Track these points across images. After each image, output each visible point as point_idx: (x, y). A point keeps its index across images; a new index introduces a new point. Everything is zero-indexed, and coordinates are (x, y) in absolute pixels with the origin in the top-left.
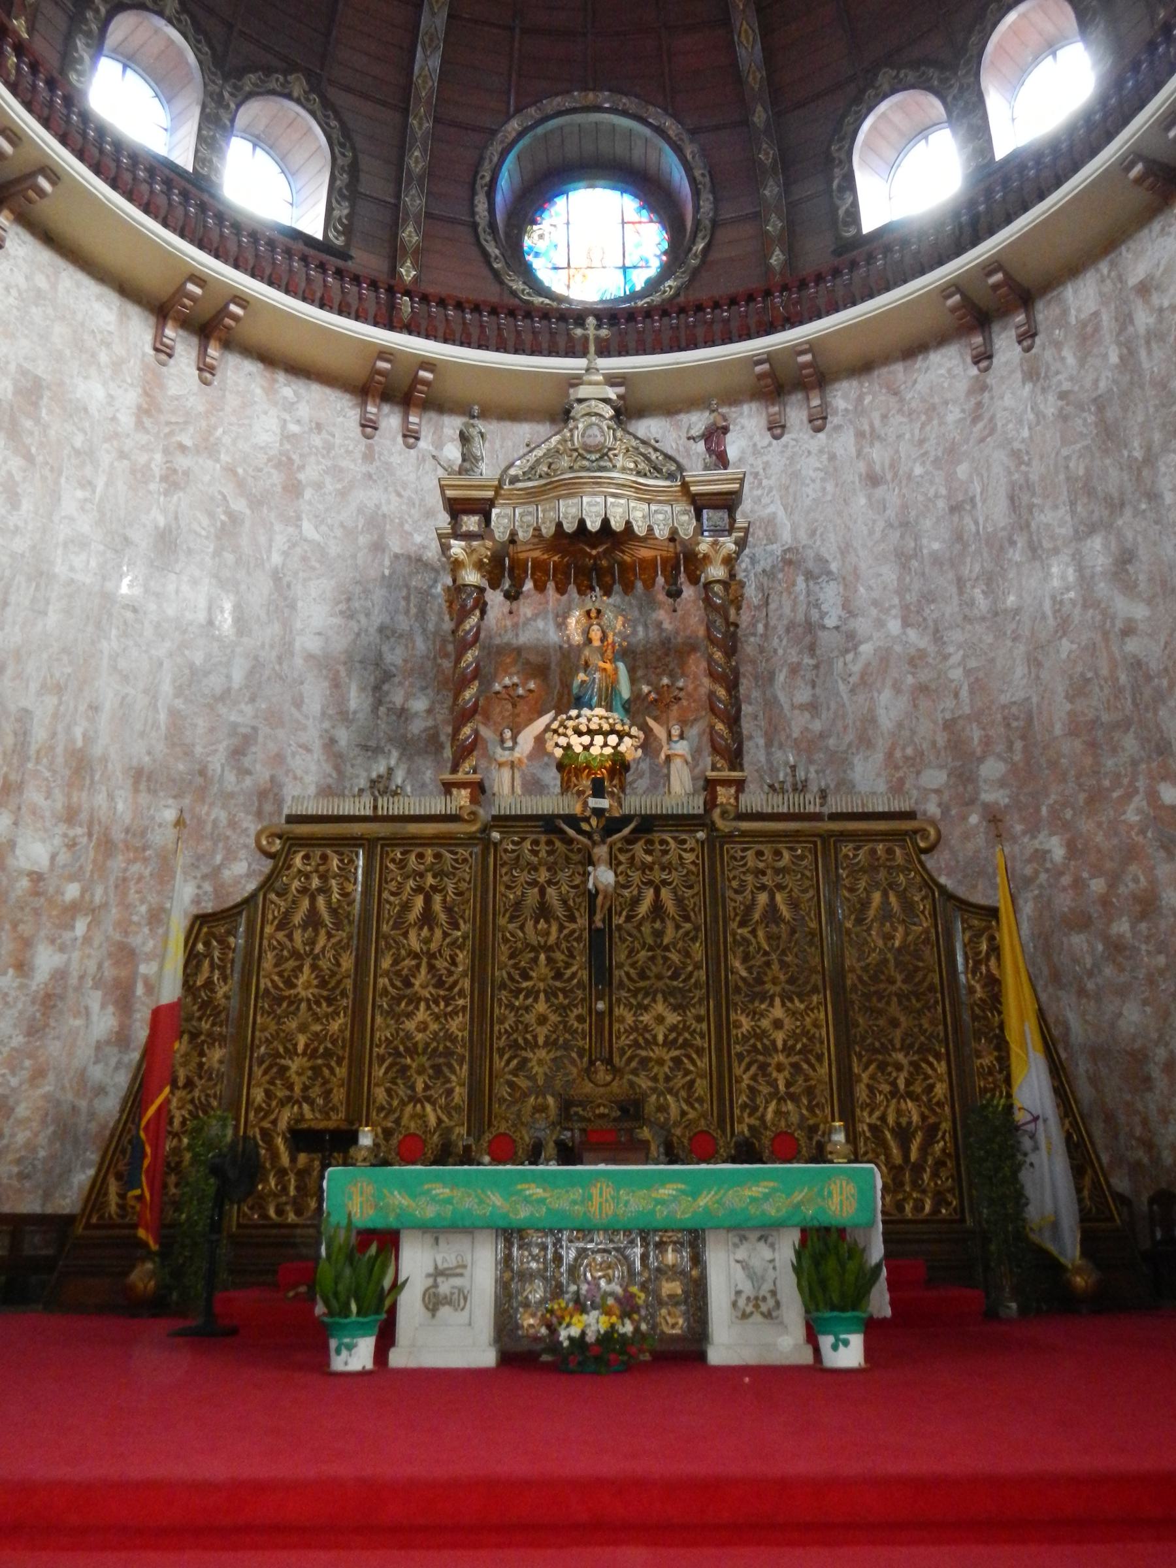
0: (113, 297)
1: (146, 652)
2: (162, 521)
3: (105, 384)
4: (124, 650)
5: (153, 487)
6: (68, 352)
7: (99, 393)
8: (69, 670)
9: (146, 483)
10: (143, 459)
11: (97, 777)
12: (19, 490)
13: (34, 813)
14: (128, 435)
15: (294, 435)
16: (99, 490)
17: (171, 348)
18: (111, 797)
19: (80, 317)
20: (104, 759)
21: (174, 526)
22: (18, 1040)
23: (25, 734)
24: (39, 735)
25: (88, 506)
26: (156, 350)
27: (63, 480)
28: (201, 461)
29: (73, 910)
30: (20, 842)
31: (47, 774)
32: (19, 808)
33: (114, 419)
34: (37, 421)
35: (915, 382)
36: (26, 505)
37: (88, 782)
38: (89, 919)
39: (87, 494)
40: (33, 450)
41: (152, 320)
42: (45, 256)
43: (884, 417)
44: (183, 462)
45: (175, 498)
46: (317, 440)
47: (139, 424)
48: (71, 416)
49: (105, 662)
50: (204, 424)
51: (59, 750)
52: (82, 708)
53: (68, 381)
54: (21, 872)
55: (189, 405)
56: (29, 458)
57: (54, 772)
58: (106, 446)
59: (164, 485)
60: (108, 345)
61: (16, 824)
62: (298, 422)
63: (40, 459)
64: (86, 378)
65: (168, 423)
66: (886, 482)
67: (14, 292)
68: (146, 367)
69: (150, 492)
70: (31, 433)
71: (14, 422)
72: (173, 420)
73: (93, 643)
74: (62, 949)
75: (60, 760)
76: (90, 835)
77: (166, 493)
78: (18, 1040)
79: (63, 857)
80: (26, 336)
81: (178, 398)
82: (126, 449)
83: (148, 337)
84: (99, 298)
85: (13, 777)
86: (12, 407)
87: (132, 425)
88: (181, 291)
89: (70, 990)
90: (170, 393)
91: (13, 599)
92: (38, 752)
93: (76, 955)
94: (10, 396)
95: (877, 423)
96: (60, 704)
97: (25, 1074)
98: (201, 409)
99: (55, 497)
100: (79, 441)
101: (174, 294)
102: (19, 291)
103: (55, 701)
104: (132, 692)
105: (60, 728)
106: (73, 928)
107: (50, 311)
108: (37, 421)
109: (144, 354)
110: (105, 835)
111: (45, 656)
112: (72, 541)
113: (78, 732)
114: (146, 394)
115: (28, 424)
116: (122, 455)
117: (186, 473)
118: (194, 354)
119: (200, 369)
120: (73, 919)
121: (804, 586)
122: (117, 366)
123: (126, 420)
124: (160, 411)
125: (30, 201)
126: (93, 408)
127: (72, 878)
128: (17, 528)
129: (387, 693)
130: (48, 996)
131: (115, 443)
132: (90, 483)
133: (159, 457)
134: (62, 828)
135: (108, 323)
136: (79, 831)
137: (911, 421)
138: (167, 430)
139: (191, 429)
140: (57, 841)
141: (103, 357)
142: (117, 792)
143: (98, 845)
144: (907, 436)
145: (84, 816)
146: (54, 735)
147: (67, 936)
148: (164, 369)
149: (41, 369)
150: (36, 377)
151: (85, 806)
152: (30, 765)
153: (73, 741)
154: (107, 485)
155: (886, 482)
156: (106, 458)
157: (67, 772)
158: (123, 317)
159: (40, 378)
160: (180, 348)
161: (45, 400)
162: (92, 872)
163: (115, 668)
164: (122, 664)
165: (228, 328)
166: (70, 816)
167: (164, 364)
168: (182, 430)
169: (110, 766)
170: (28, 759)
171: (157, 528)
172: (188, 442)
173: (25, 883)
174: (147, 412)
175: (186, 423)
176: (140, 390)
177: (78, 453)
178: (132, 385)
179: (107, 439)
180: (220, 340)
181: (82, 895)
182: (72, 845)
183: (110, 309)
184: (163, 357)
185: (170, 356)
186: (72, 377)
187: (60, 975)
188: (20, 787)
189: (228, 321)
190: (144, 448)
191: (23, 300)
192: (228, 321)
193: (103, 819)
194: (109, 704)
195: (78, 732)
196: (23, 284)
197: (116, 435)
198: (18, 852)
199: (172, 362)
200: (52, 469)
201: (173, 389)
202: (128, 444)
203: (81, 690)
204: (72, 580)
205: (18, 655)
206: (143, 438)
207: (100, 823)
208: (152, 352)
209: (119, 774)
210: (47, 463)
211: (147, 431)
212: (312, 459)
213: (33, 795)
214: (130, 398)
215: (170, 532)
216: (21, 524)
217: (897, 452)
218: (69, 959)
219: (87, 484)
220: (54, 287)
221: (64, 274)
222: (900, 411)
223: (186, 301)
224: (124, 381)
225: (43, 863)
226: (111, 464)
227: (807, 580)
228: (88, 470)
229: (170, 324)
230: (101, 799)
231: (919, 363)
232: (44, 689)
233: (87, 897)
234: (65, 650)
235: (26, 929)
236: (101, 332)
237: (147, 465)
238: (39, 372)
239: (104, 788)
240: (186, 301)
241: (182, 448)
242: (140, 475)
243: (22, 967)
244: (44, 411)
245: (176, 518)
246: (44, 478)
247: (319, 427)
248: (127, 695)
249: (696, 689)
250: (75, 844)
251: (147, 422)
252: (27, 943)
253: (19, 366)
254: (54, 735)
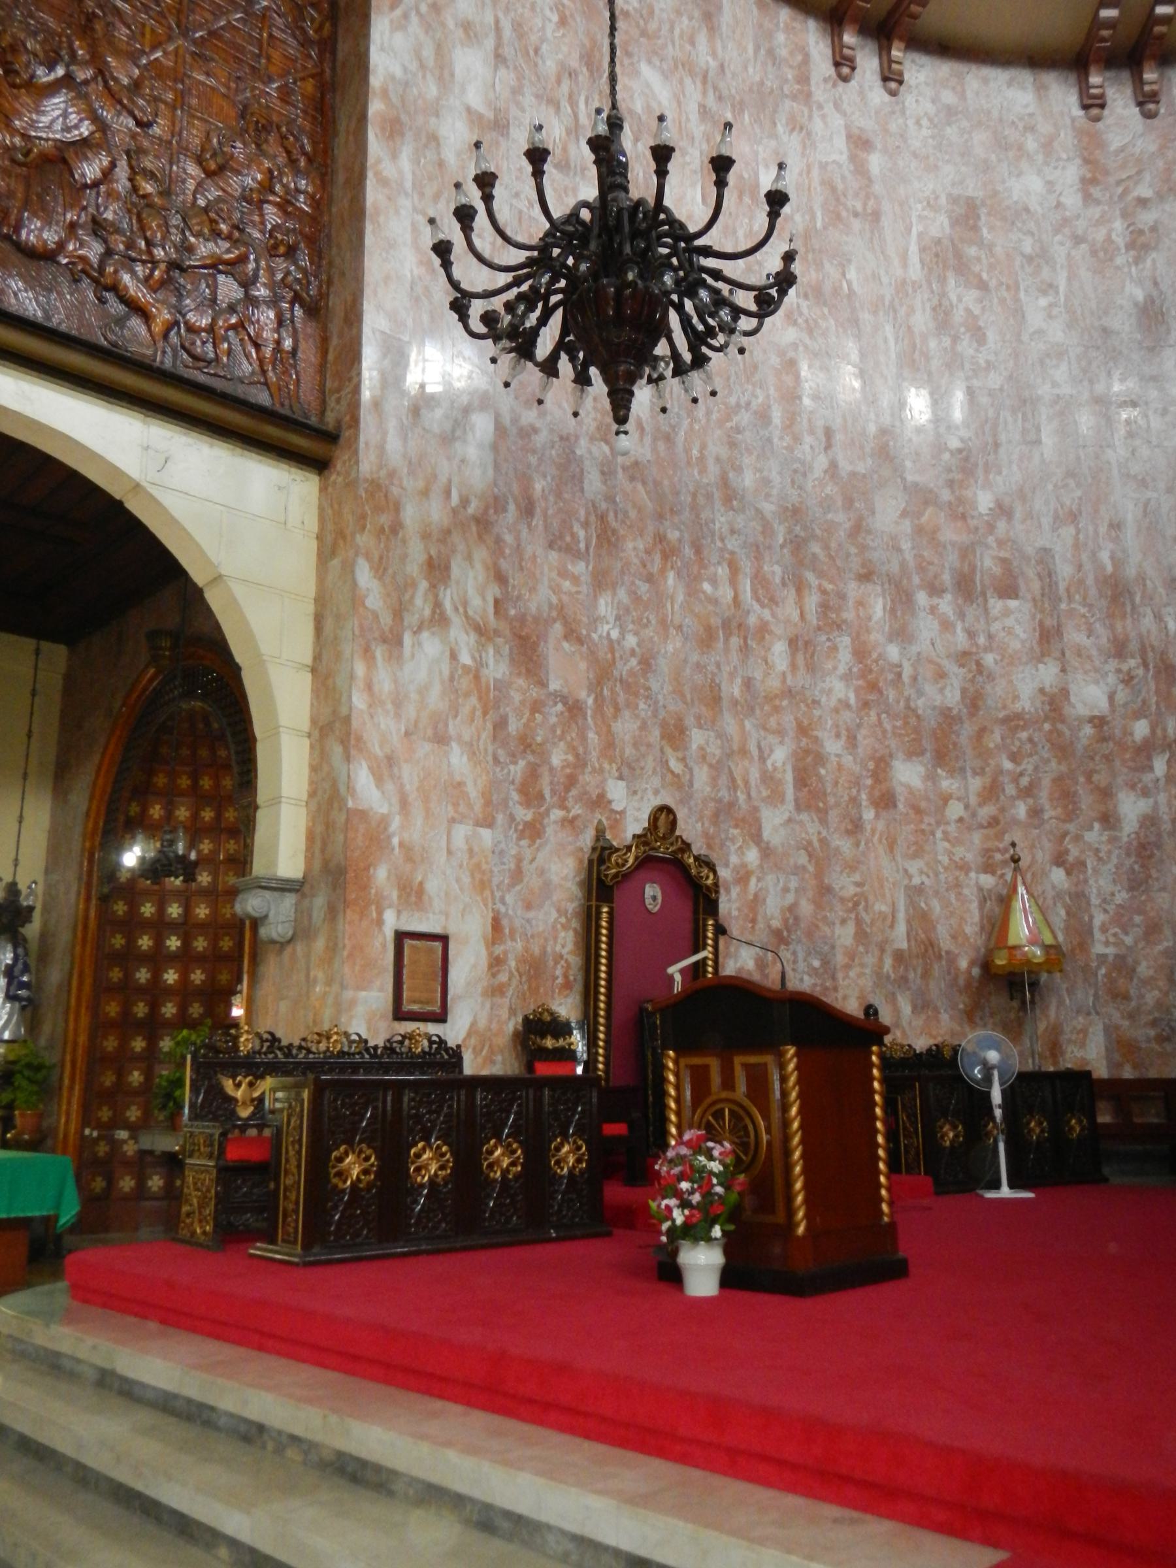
0: (1025, 76)
1: (1158, 446)
2: (1140, 295)
3: (1039, 172)
4: (1133, 452)
5: (1119, 261)
6: (993, 157)
7: (1035, 183)
8: (1079, 493)
9: (1111, 260)
10: (1100, 235)
11: (1138, 599)
12: (981, 323)
13: (1080, 656)
14: (1078, 217)
16: (1062, 289)
17: (1102, 96)
18: (1158, 617)
19: (995, 114)
20: (1142, 578)
21: (1155, 293)
22: (1122, 897)
23: (1050, 575)
24: (1064, 571)
25: (1055, 311)
26: (1085, 107)
27: (1022, 295)
28: (1167, 207)
29: (1146, 750)
30: (1073, 688)
31: (1083, 610)
32: (1063, 654)
33: (1059, 205)
34: (980, 243)
36: (991, 336)
37: (1128, 609)
38: (1167, 756)
39: (1051, 299)
40: (985, 276)
41: (1072, 78)
42: (945, 68)
44: (1146, 218)
45: (1149, 263)
47: (1087, 198)
48: (1013, 223)
49: (1115, 472)
50: (1160, 164)
51: (1090, 581)
52: (1103, 530)
53: (1000, 188)
54: (1081, 720)
55: (1137, 150)
56: (983, 286)
57: (1090, 606)
58: (1059, 238)
59: (1132, 253)
60: (1031, 129)
61: (1063, 670)
63: (993, 283)
64: (1019, 175)
65: (1119, 183)
67: (925, 122)
68: (1080, 133)
69: (1118, 268)
70: (979, 259)
71: (958, 255)
72: (1124, 176)
73: (1097, 457)
74: (1145, 793)
75: (1093, 592)
76: (1145, 665)
77: (1137, 261)
78: (1122, 897)
79: (1122, 696)
80: (948, 161)
81: (1122, 149)
82: (1080, 232)
83: (1073, 99)
84: (1010, 84)
85: (1049, 622)
86: (952, 241)
87: (1080, 203)
88: (1097, 23)
89: (1165, 836)
90: (1112, 148)
91: (1003, 438)
92: (1068, 590)
93: (1162, 798)
94: (948, 230)
96: (1078, 532)
97: (1139, 931)
98: (1153, 148)
99: (1018, 313)
100: (1028, 246)
101: (1090, 30)
102: (931, 120)
103: (1072, 530)
104: (1155, 495)
105: (1084, 557)
106: (1151, 769)
107: (965, 124)
108: (980, 243)
109: (1073, 120)
110: (1162, 660)
111: (1050, 487)
112: (1048, 355)
113: (1105, 556)
114: (1086, 161)
115: (972, 251)
116: (1078, 240)
117: (1154, 229)
118: (1129, 91)
119: (1140, 104)
120: (1149, 758)
122: (1047, 146)
123: (1072, 200)
124: (1107, 173)
125: (915, 17)
126: (1034, 206)
127: (1138, 715)
128: (988, 362)
130: (1143, 846)
131: (1066, 231)
132: (1051, 286)
133: (1118, 225)
134: (1113, 664)
135: (1026, 106)
136: (1132, 663)
138: (1120, 190)
139: (1147, 177)
140: (1112, 679)
141: (1031, 144)
142: (1164, 611)
143: (1158, 672)
145: (1134, 646)
146: (1080, 567)
147: (1147, 778)
148: (1100, 125)
149: (973, 189)
150: (968, 198)
151: (1133, 635)
152: (1063, 606)
153: (1102, 567)
154: (1069, 279)
156: (1060, 250)
157: (1104, 603)
158: (1041, 89)
159: (972, 198)
160: (1111, 93)
161: (983, 218)
162: (1157, 704)
163: (1128, 475)
164: (1135, 468)
165: (1161, 37)
166: (1119, 649)
167: (1097, 119)
168: (1136, 183)
169: (1148, 582)
170: (1060, 600)
171: (1136, 304)
172: (1144, 191)
173: (1088, 730)
174: (1094, 181)
175: (1139, 172)
176: (1078, 161)
177: (1030, 259)
178: (1068, 159)
179: (1057, 231)
180: (1154, 57)
181: (1153, 731)
182: (1128, 680)
183: (1024, 89)
184: (1095, 111)
185: (1102, 106)
186: (1004, 182)
187: (1149, 821)
188: (1059, 631)
189: (1158, 29)
190: (1102, 220)
191: (935, 126)
192: (1158, 29)
193: (1156, 644)
194: (1130, 514)
195: (1105, 556)
196: (930, 108)
197: (1066, 221)
198: (1073, 699)
199: (1106, 112)
200: (1008, 288)
201: (1115, 141)
202: (1081, 226)
203: (1096, 511)
204: (1058, 395)
205: (1022, 495)
206: (1095, 212)
207: (1153, 648)
208: (1081, 113)
209: (1161, 590)
210: (1002, 284)
211: (1098, 202)
213: (1075, 636)
214: (1071, 173)
215: (1153, 302)
216: (992, 358)
218: (1156, 803)
219: (1048, 288)
220: (963, 97)
221: (969, 78)
223: (1105, 33)
224: (1059, 159)
225: (1103, 705)
226: (1069, 255)
228: (1046, 273)
229: (1093, 70)
230: (1148, 622)
232: (1057, 521)
233: (1159, 732)
234: (1070, 474)
235: (1101, 779)
236: (1021, 119)
237: (1109, 239)
238: (970, 192)
239: (1149, 611)
240: (1105, 33)
241: (1143, 202)
242: (1103, 254)
243: (1109, 820)
244: (985, 231)
245: (1156, 284)
246: (1002, 301)
248: (1149, 500)
250: (1132, 678)
251: (1096, 192)
252: (1106, 793)
253: (949, 195)
254: (1080, 567)
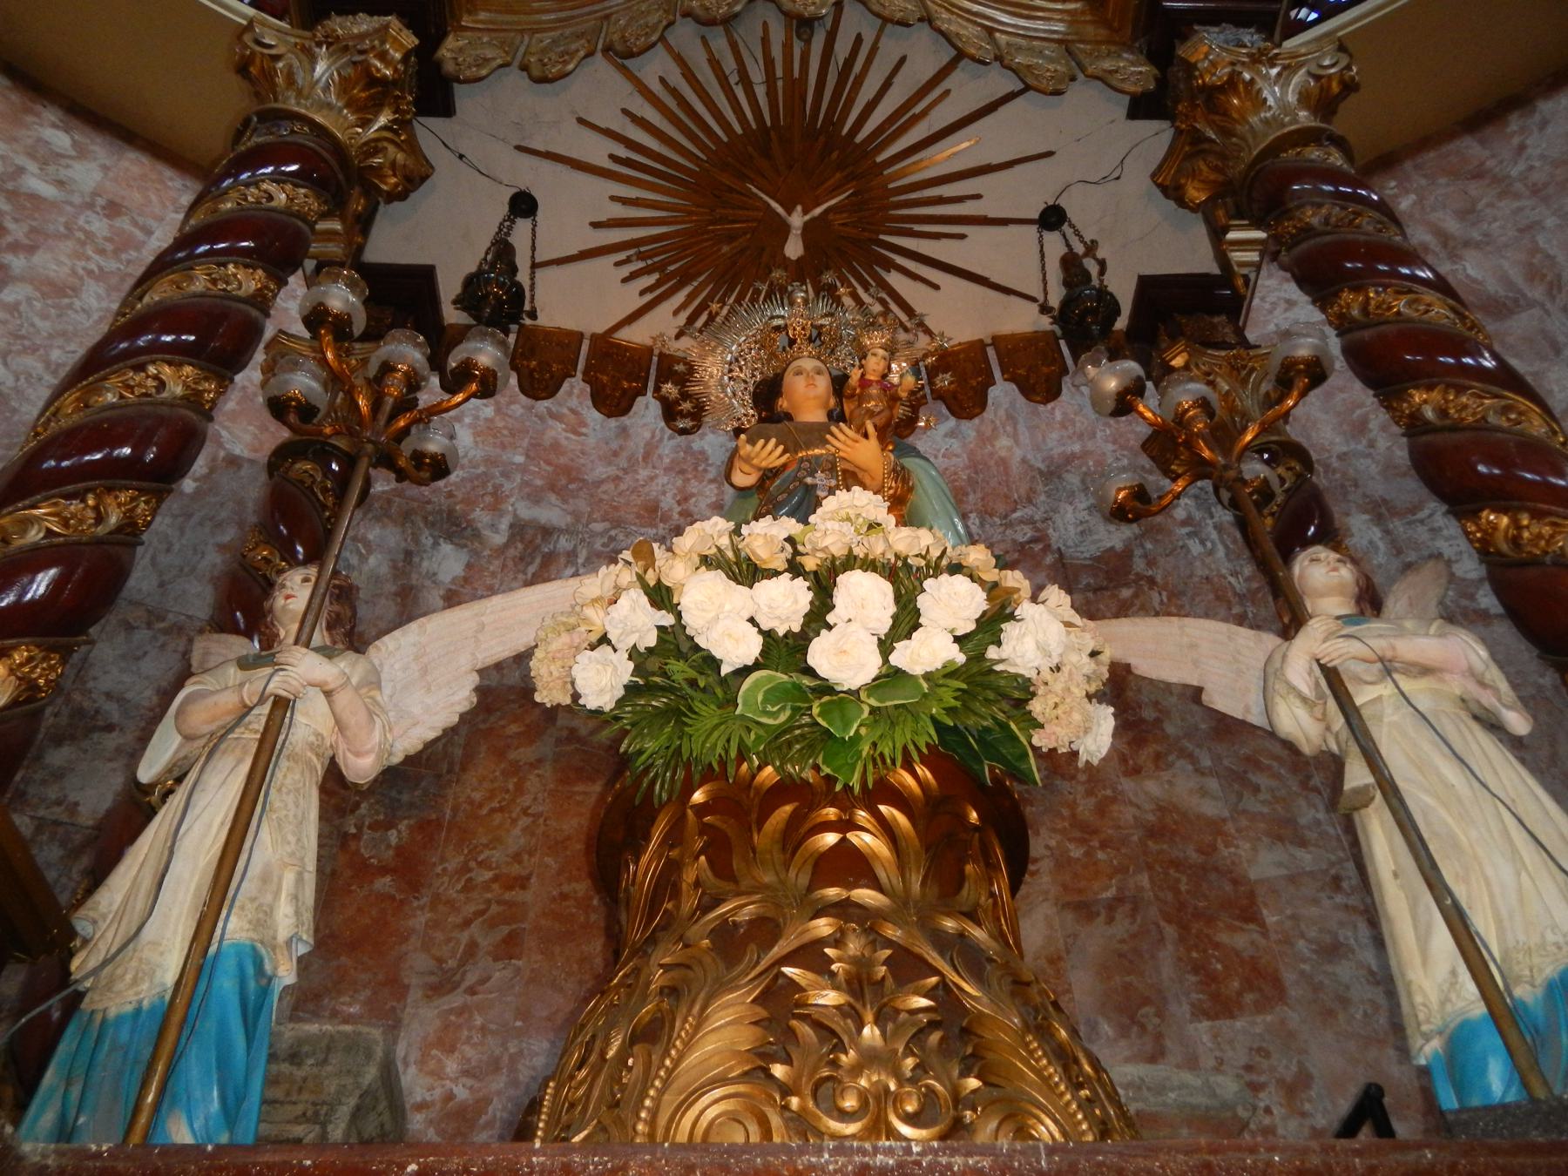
15: (34, 197)
35: (1522, 148)
43: (1468, 213)
46: (99, 225)
62: (60, 183)
66: (1532, 304)
95: (1452, 225)
121: (1376, 533)
129: (59, 775)
137: (1546, 200)
144: (1550, 222)
155: (1532, 304)
212: (70, 245)
217: (1535, 250)
222: (1502, 195)
227: (1379, 519)
231: (1514, 122)
247: (113, 209)
249: (1101, 809)
